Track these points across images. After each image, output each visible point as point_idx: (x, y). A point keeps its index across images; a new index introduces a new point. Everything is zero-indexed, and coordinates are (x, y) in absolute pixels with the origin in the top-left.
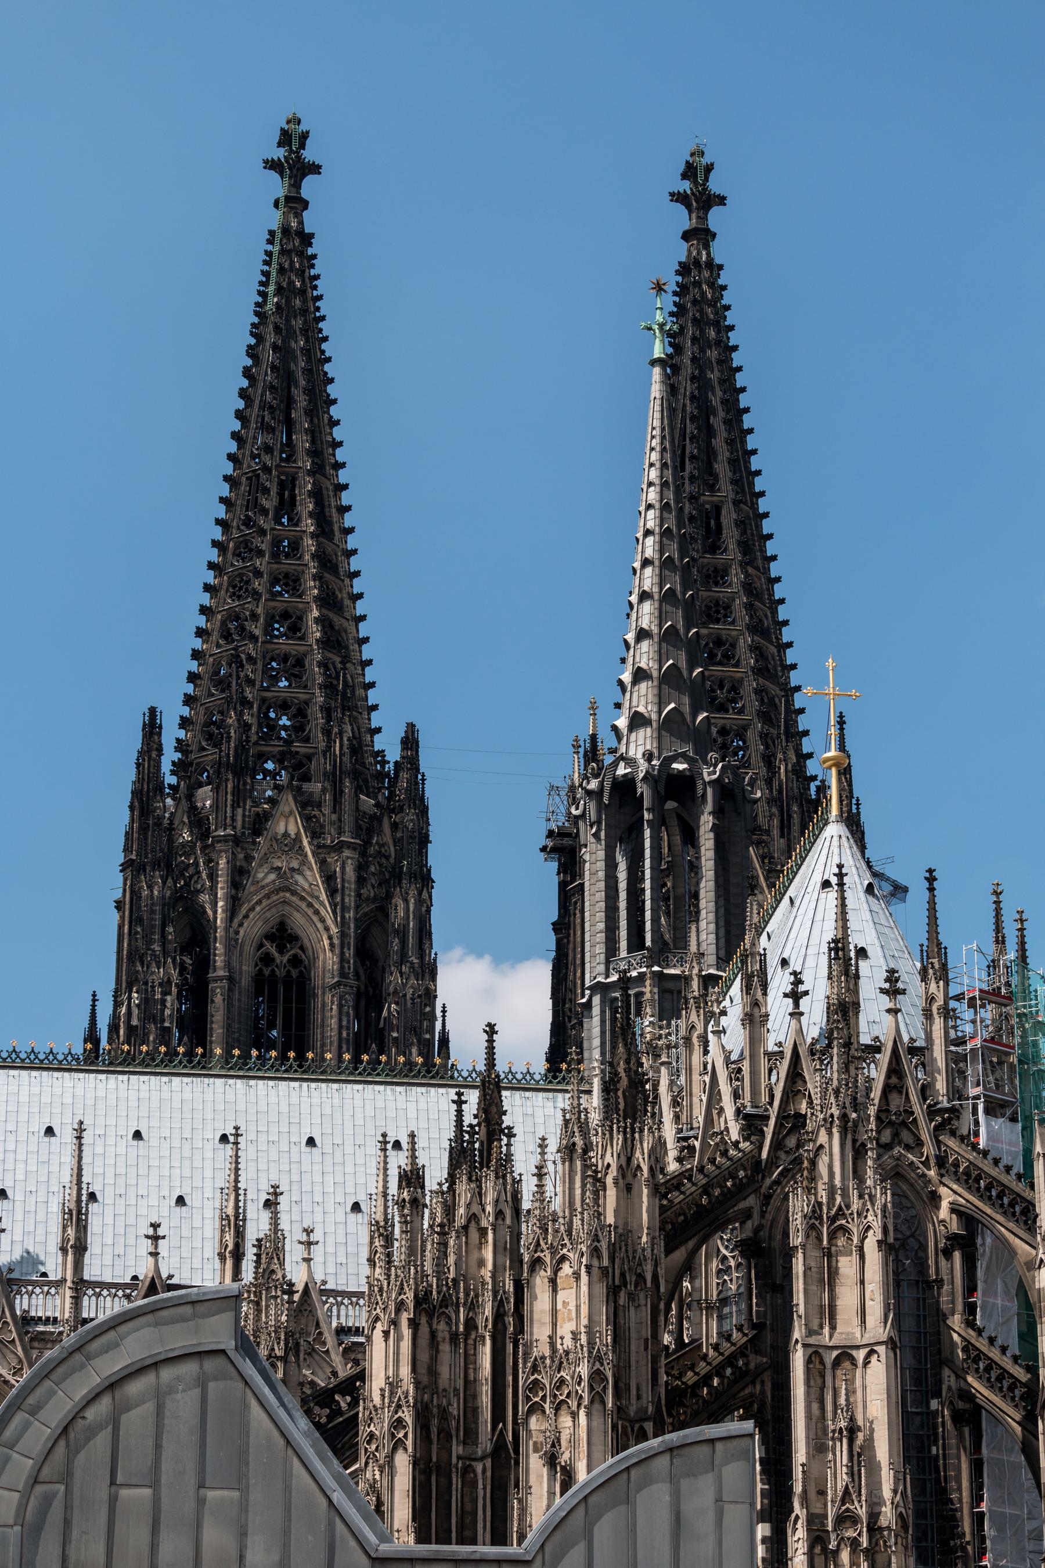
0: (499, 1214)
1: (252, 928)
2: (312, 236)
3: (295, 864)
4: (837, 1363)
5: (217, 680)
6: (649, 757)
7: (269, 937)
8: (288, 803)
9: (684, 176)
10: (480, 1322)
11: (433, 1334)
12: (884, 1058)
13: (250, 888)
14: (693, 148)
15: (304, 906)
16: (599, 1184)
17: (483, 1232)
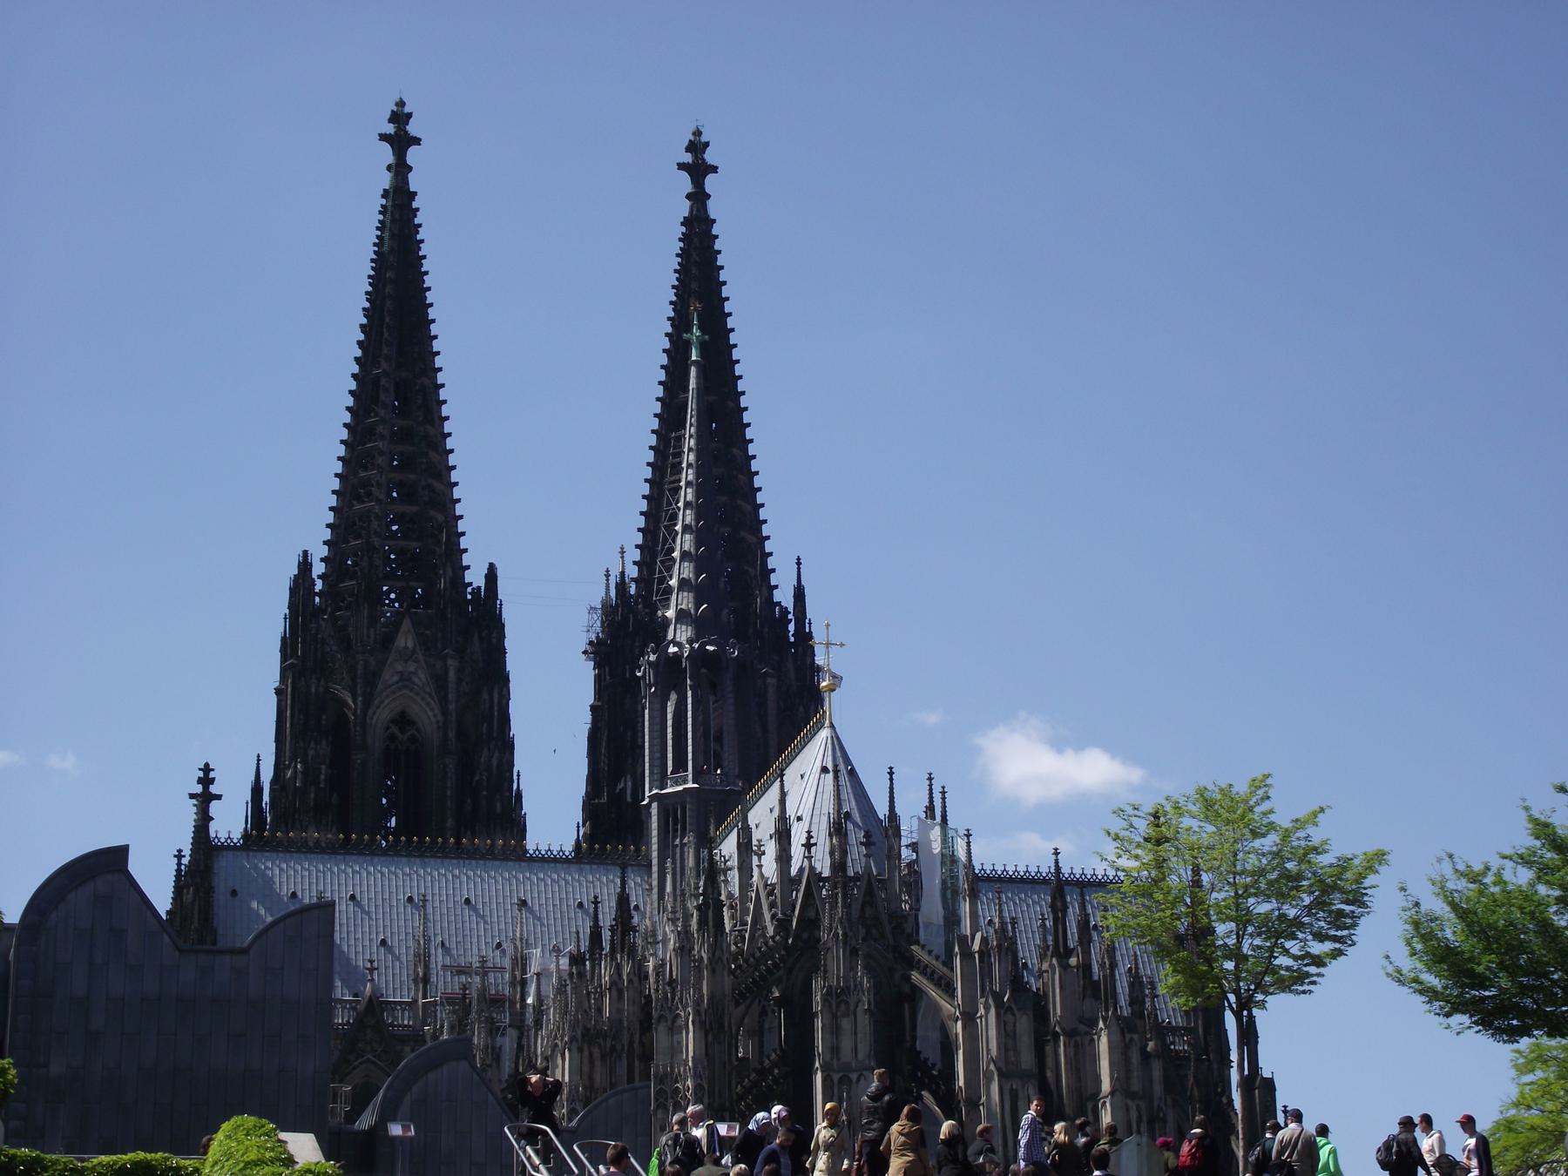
0: (630, 981)
1: (382, 715)
2: (415, 193)
3: (412, 669)
4: (840, 1081)
5: (348, 523)
6: (690, 642)
7: (393, 721)
8: (406, 624)
9: (688, 150)
10: (619, 1047)
11: (591, 1055)
12: (861, 884)
13: (380, 686)
14: (693, 128)
15: (418, 699)
16: (699, 970)
17: (620, 992)
